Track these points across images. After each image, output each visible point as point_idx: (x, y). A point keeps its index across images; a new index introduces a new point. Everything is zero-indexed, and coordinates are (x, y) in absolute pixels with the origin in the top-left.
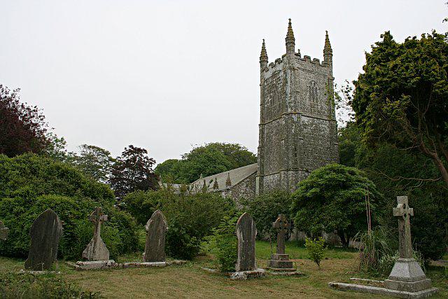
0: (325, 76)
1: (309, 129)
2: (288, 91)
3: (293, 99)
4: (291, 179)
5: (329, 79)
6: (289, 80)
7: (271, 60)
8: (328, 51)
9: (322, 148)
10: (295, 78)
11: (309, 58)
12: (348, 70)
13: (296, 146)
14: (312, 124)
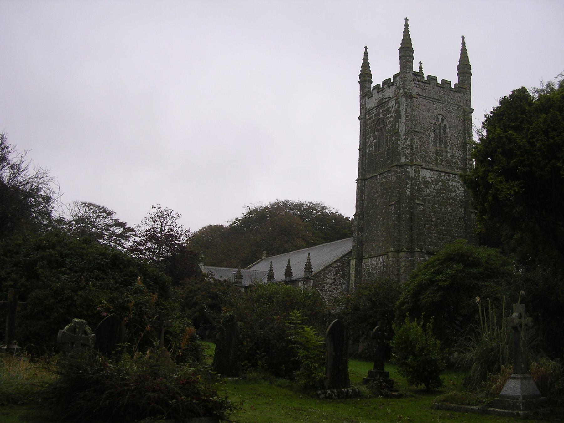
0: (458, 107)
1: (432, 190)
2: (402, 129)
3: (408, 143)
4: (403, 264)
5: (464, 112)
6: (403, 113)
7: (377, 80)
8: (464, 69)
9: (451, 218)
10: (413, 110)
11: (435, 79)
12: (483, 103)
13: (412, 214)
14: (437, 182)
